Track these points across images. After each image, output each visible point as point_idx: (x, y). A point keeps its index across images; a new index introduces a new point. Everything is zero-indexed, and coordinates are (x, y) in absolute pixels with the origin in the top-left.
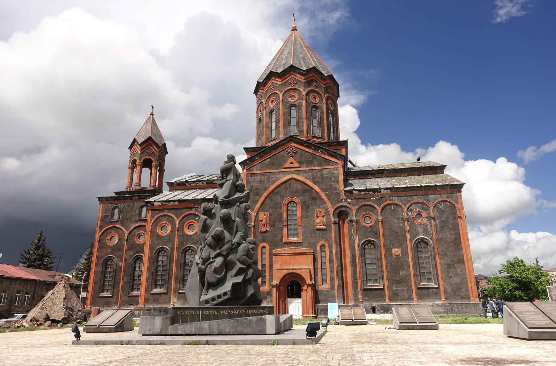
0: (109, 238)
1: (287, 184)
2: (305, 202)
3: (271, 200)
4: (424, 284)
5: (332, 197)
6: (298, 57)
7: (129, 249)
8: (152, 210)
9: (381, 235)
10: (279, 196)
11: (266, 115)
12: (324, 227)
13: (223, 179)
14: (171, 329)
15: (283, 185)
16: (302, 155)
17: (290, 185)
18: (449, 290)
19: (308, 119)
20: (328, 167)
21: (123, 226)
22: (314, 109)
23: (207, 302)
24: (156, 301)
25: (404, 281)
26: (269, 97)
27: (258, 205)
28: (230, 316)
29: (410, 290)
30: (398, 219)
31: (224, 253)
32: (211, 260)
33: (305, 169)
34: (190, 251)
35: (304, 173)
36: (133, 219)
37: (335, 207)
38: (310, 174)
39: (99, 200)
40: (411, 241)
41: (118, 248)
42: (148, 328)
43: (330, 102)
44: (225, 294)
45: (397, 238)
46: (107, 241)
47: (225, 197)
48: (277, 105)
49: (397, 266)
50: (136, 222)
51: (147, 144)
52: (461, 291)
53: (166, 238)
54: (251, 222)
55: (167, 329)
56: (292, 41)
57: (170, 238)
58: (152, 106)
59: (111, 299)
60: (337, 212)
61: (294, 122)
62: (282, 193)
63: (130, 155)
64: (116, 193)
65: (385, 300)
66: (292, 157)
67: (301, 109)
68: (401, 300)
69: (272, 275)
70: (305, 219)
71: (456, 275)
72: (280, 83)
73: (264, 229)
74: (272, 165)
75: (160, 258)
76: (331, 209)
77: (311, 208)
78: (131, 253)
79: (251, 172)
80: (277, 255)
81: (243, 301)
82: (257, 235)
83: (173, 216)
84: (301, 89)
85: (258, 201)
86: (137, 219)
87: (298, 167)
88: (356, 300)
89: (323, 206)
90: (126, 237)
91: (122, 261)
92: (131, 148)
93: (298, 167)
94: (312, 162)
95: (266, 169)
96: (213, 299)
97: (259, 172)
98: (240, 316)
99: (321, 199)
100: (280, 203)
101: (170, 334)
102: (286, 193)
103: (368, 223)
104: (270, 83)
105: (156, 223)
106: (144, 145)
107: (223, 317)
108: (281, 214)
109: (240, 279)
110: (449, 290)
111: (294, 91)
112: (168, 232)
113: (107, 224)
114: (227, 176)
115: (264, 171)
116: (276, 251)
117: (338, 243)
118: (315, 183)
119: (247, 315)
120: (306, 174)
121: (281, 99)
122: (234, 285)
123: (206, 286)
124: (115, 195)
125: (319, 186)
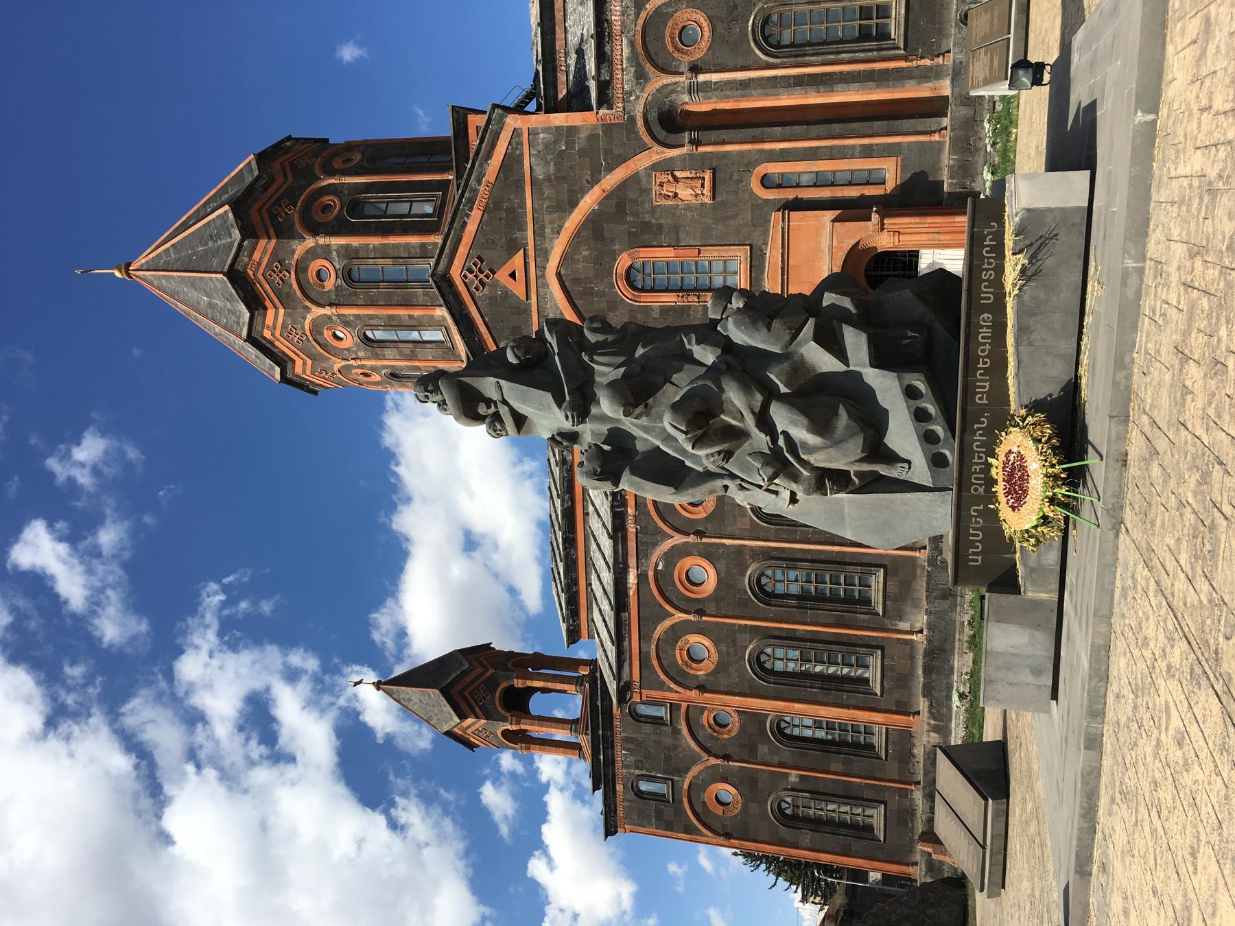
0: (719, 810)
1: (575, 290)
2: (630, 234)
5: (616, 151)
6: (204, 257)
11: (377, 357)
12: (708, 175)
13: (497, 417)
14: (1037, 592)
15: (579, 303)
17: (577, 281)
19: (386, 230)
21: (687, 770)
23: (937, 461)
31: (759, 398)
32: (781, 442)
35: (543, 236)
36: (668, 741)
37: (647, 139)
38: (547, 218)
42: (1026, 677)
44: (911, 393)
46: (729, 815)
47: (559, 402)
48: (346, 323)
50: (677, 732)
51: (459, 700)
55: (1036, 604)
56: (159, 278)
60: (661, 134)
62: (604, 305)
66: (494, 273)
67: (357, 250)
70: (682, 235)
72: (282, 311)
75: (779, 666)
77: (647, 217)
78: (763, 750)
81: (939, 328)
89: (644, 181)
90: (719, 761)
91: (787, 775)
96: (929, 438)
99: (623, 186)
101: (1055, 597)
102: (602, 294)
104: (282, 345)
105: (680, 678)
109: (856, 342)
112: (707, 642)
113: (680, 812)
114: (489, 402)
118: (573, 204)
120: (548, 231)
121: (327, 311)
122: (879, 360)
123: (882, 470)
125: (584, 192)
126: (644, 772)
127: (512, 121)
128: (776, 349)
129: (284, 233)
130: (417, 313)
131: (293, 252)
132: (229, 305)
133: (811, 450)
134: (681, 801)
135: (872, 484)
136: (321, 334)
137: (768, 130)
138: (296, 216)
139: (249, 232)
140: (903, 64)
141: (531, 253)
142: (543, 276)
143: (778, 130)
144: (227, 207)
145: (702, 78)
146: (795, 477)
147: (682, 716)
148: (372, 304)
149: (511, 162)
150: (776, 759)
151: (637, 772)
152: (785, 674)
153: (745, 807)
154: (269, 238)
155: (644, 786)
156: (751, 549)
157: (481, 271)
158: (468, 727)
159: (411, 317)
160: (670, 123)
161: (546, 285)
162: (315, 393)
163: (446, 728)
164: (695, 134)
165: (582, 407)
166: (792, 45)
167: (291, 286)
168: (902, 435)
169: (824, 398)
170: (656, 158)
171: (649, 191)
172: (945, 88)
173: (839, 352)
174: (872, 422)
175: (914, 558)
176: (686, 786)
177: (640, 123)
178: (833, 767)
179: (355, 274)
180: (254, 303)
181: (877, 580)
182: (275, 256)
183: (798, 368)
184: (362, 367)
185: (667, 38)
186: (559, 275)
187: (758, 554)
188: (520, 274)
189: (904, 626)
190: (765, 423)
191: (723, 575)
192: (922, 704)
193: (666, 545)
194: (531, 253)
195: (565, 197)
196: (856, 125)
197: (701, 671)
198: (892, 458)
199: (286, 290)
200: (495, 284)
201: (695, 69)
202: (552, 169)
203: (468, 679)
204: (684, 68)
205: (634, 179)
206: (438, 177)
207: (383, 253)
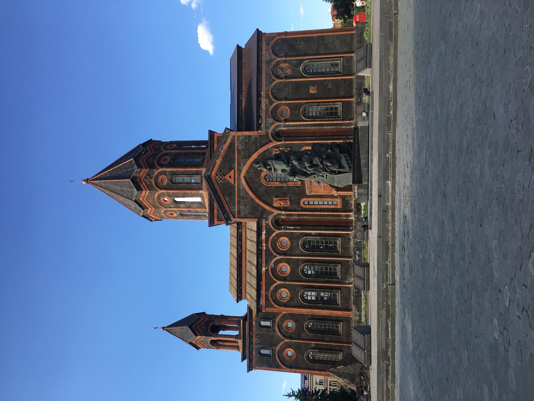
9: (298, 102)
17: (250, 179)
19: (185, 166)
20: (236, 145)
22: (176, 161)
23: (350, 167)
26: (160, 204)
27: (267, 207)
28: (359, 151)
30: (285, 87)
33: (236, 165)
35: (240, 166)
36: (271, 334)
37: (272, 139)
38: (242, 160)
39: (252, 370)
42: (364, 197)
43: (168, 147)
44: (345, 157)
47: (284, 163)
48: (169, 195)
50: (274, 330)
51: (195, 330)
61: (187, 179)
63: (205, 349)
64: (243, 359)
68: (352, 88)
69: (328, 195)
75: (309, 298)
78: (303, 335)
84: (156, 173)
87: (234, 171)
92: (198, 348)
93: (234, 171)
95: (235, 200)
96: (348, 164)
97: (236, 206)
98: (358, 147)
104: (145, 203)
106: (197, 332)
107: (359, 155)
113: (275, 360)
114: (269, 165)
115: (236, 201)
119: (358, 142)
120: (242, 164)
123: (341, 170)
127: (233, 133)
129: (152, 166)
131: (154, 173)
132: (129, 190)
133: (330, 167)
135: (340, 173)
138: (155, 162)
140: (342, 122)
141: (236, 170)
142: (240, 177)
143: (308, 138)
145: (287, 123)
146: (327, 171)
147: (276, 325)
149: (232, 144)
153: (297, 356)
155: (263, 351)
156: (301, 259)
158: (198, 340)
161: (240, 180)
162: (152, 221)
165: (288, 163)
168: (344, 162)
170: (274, 145)
177: (270, 135)
180: (139, 189)
181: (339, 268)
182: (148, 174)
186: (244, 177)
190: (321, 163)
192: (353, 307)
194: (236, 170)
200: (225, 179)
203: (198, 322)
205: (268, 150)
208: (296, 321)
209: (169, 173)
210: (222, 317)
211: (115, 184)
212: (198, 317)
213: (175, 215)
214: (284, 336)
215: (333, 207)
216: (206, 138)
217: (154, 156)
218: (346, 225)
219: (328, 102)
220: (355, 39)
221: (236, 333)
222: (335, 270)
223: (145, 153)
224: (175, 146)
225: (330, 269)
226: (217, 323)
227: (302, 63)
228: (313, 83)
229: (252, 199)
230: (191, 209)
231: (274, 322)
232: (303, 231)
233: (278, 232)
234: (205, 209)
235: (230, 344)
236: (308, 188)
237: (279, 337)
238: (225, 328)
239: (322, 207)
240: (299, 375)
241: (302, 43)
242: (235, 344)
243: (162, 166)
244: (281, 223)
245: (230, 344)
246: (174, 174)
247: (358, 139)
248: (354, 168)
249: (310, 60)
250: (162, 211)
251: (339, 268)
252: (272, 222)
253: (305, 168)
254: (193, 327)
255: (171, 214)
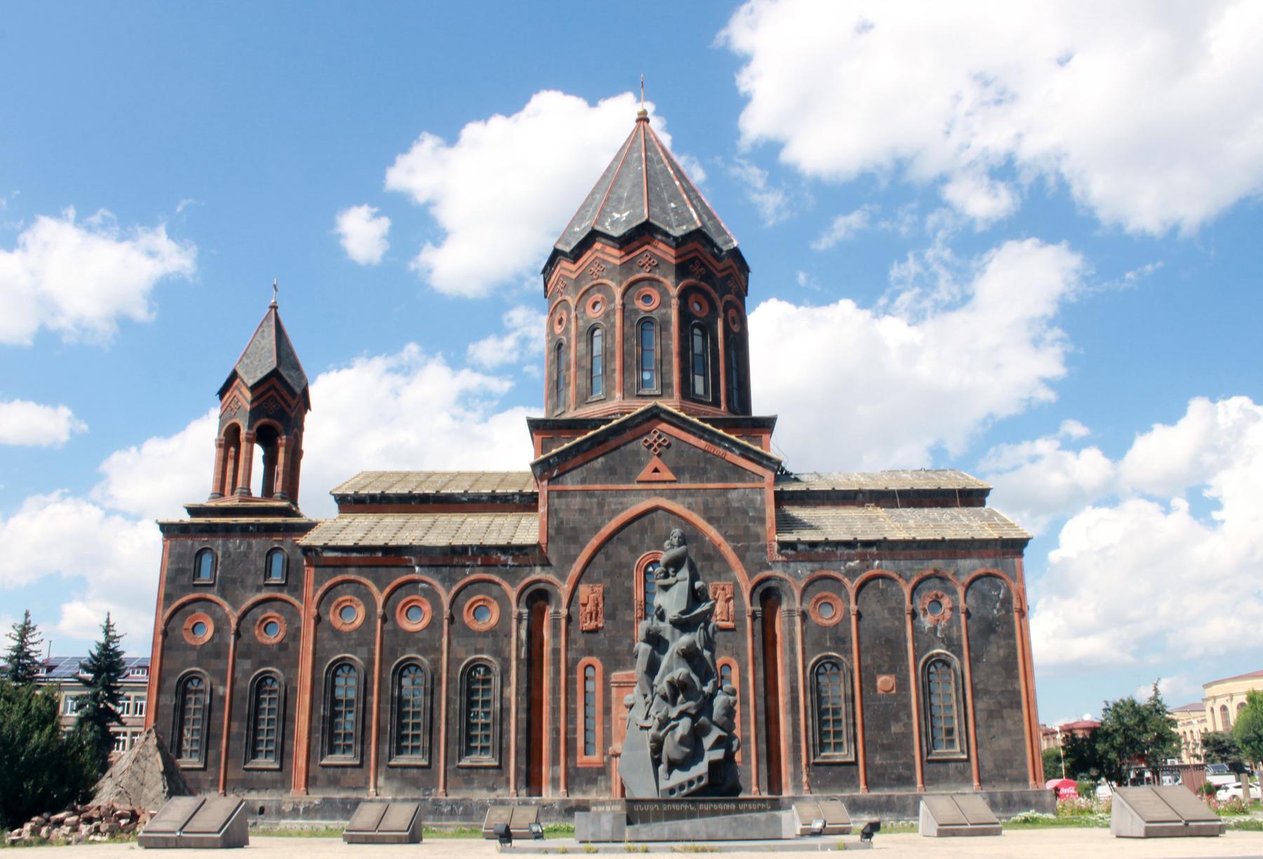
0: (188, 625)
1: (645, 520)
3: (608, 557)
4: (941, 752)
5: (748, 555)
7: (240, 654)
8: (316, 566)
10: (626, 548)
11: (578, 336)
12: (730, 624)
15: (636, 524)
16: (680, 453)
17: (652, 522)
18: (989, 764)
20: (739, 485)
21: (224, 597)
22: (696, 331)
23: (672, 791)
24: (334, 783)
25: (900, 745)
26: (587, 291)
28: (714, 813)
29: (911, 767)
30: (892, 611)
32: (673, 723)
33: (688, 485)
34: (413, 669)
35: (685, 496)
36: (250, 580)
38: (700, 500)
40: (916, 660)
41: (214, 651)
42: (591, 829)
43: (732, 313)
44: (700, 778)
45: (886, 650)
46: (185, 633)
47: (683, 613)
48: (608, 315)
49: (884, 714)
50: (259, 589)
51: (267, 386)
52: (1011, 767)
53: (354, 636)
54: (558, 605)
55: (623, 832)
57: (363, 636)
58: (275, 286)
59: (201, 774)
60: (759, 590)
62: (634, 542)
65: (858, 787)
66: (659, 455)
68: (891, 786)
69: (610, 729)
71: (1005, 732)
73: (593, 625)
74: (610, 472)
76: (746, 587)
78: (246, 664)
79: (559, 487)
80: (621, 685)
82: (572, 636)
83: (369, 582)
85: (574, 558)
86: (261, 581)
88: (797, 785)
91: (224, 683)
92: (222, 393)
94: (705, 471)
95: (595, 482)
96: (681, 787)
97: (580, 487)
99: (723, 559)
100: (629, 566)
102: (642, 541)
103: (827, 618)
104: (588, 256)
106: (261, 390)
107: (703, 814)
108: (630, 591)
109: (719, 754)
110: (989, 764)
111: (651, 286)
113: (185, 589)
114: (676, 572)
116: (617, 675)
117: (760, 660)
118: (710, 520)
119: (738, 811)
120: (690, 500)
121: (618, 300)
122: (712, 765)
124: (187, 518)
125: (719, 528)
126: (220, 560)
128: (715, 718)
129: (682, 270)
130: (617, 376)
131: (665, 277)
133: (672, 736)
134: (194, 592)
135: (656, 763)
136: (599, 291)
137: (762, 668)
139: (680, 242)
142: (656, 495)
144: (699, 224)
145: (798, 620)
146: (660, 729)
148: (625, 339)
150: (238, 675)
151: (220, 553)
152: (334, 687)
153: (193, 648)
154: (676, 258)
156: (440, 659)
157: (660, 445)
159: (614, 371)
160: (768, 596)
161: (649, 497)
162: (544, 271)
163: (241, 372)
164: (759, 614)
165: (683, 625)
166: (818, 683)
167: (638, 272)
169: (694, 740)
170: (743, 585)
171: (719, 579)
172: (787, 793)
173: (713, 748)
174: (683, 764)
175: (437, 786)
176: (210, 596)
177: (767, 573)
178: (235, 725)
179: (647, 326)
181: (418, 759)
183: (705, 731)
184: (569, 320)
185: (825, 594)
187: (436, 663)
188: (657, 476)
189: (381, 781)
190: (682, 714)
191: (417, 636)
193: (441, 590)
195: (715, 514)
196: (763, 732)
197: (333, 617)
198: (670, 771)
199: (636, 268)
200: (649, 457)
201: (804, 616)
202: (735, 504)
203: (284, 392)
204: (805, 606)
205: (728, 568)
206: (723, 398)
207: (665, 352)
208: (282, 646)
209: (665, 314)
210: (295, 454)
211: (636, 185)
212: (298, 390)
213: (558, 329)
214: (245, 614)
215: (580, 743)
216: (757, 410)
217: (708, 277)
218: (532, 781)
219: (854, 724)
220: (1016, 789)
221: (257, 488)
222: (415, 749)
223: (714, 255)
224: (736, 328)
225: (416, 737)
226: (282, 440)
227: (953, 652)
228: (902, 685)
229: (597, 529)
230: (573, 370)
231: (279, 587)
232: (514, 663)
233: (513, 594)
234: (573, 407)
235: (229, 473)
236: (627, 676)
237: (243, 602)
238: (270, 461)
239: (580, 715)
240: (147, 654)
241: (1002, 652)
242: (228, 487)
243: (683, 296)
244: (535, 606)
245: (229, 473)
246: (664, 325)
247: (747, 811)
248: (667, 801)
249: (959, 673)
250: (568, 298)
251: (418, 759)
252: (539, 581)
253: (669, 669)
254: (274, 381)
255: (560, 321)
